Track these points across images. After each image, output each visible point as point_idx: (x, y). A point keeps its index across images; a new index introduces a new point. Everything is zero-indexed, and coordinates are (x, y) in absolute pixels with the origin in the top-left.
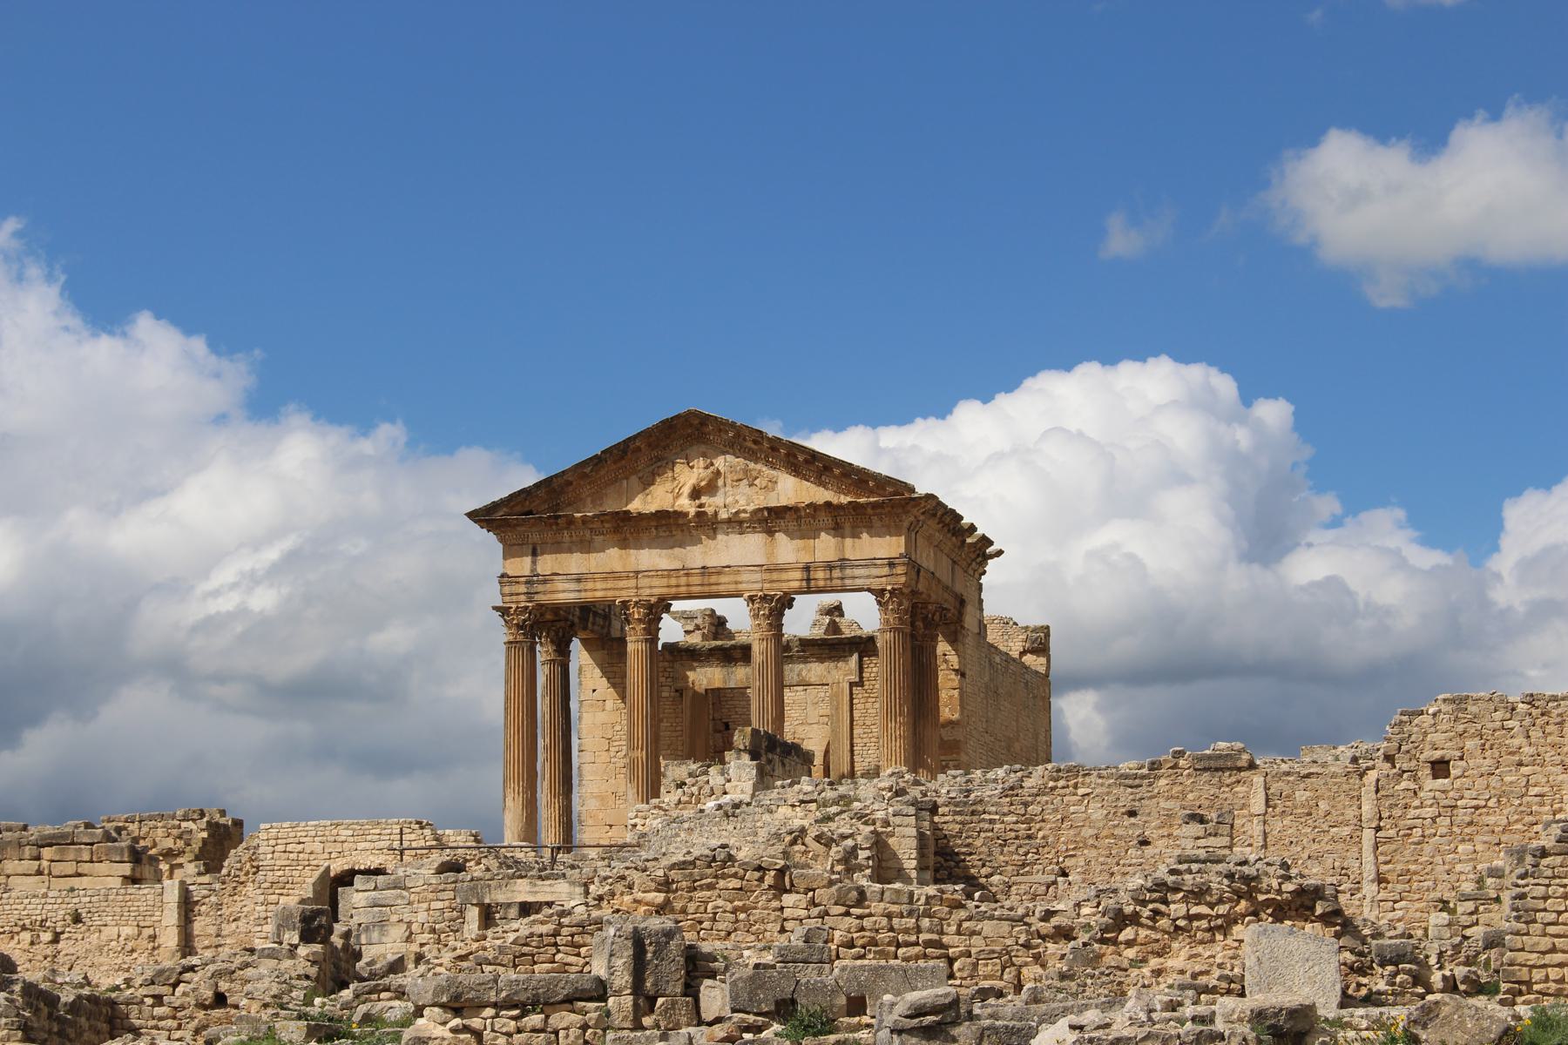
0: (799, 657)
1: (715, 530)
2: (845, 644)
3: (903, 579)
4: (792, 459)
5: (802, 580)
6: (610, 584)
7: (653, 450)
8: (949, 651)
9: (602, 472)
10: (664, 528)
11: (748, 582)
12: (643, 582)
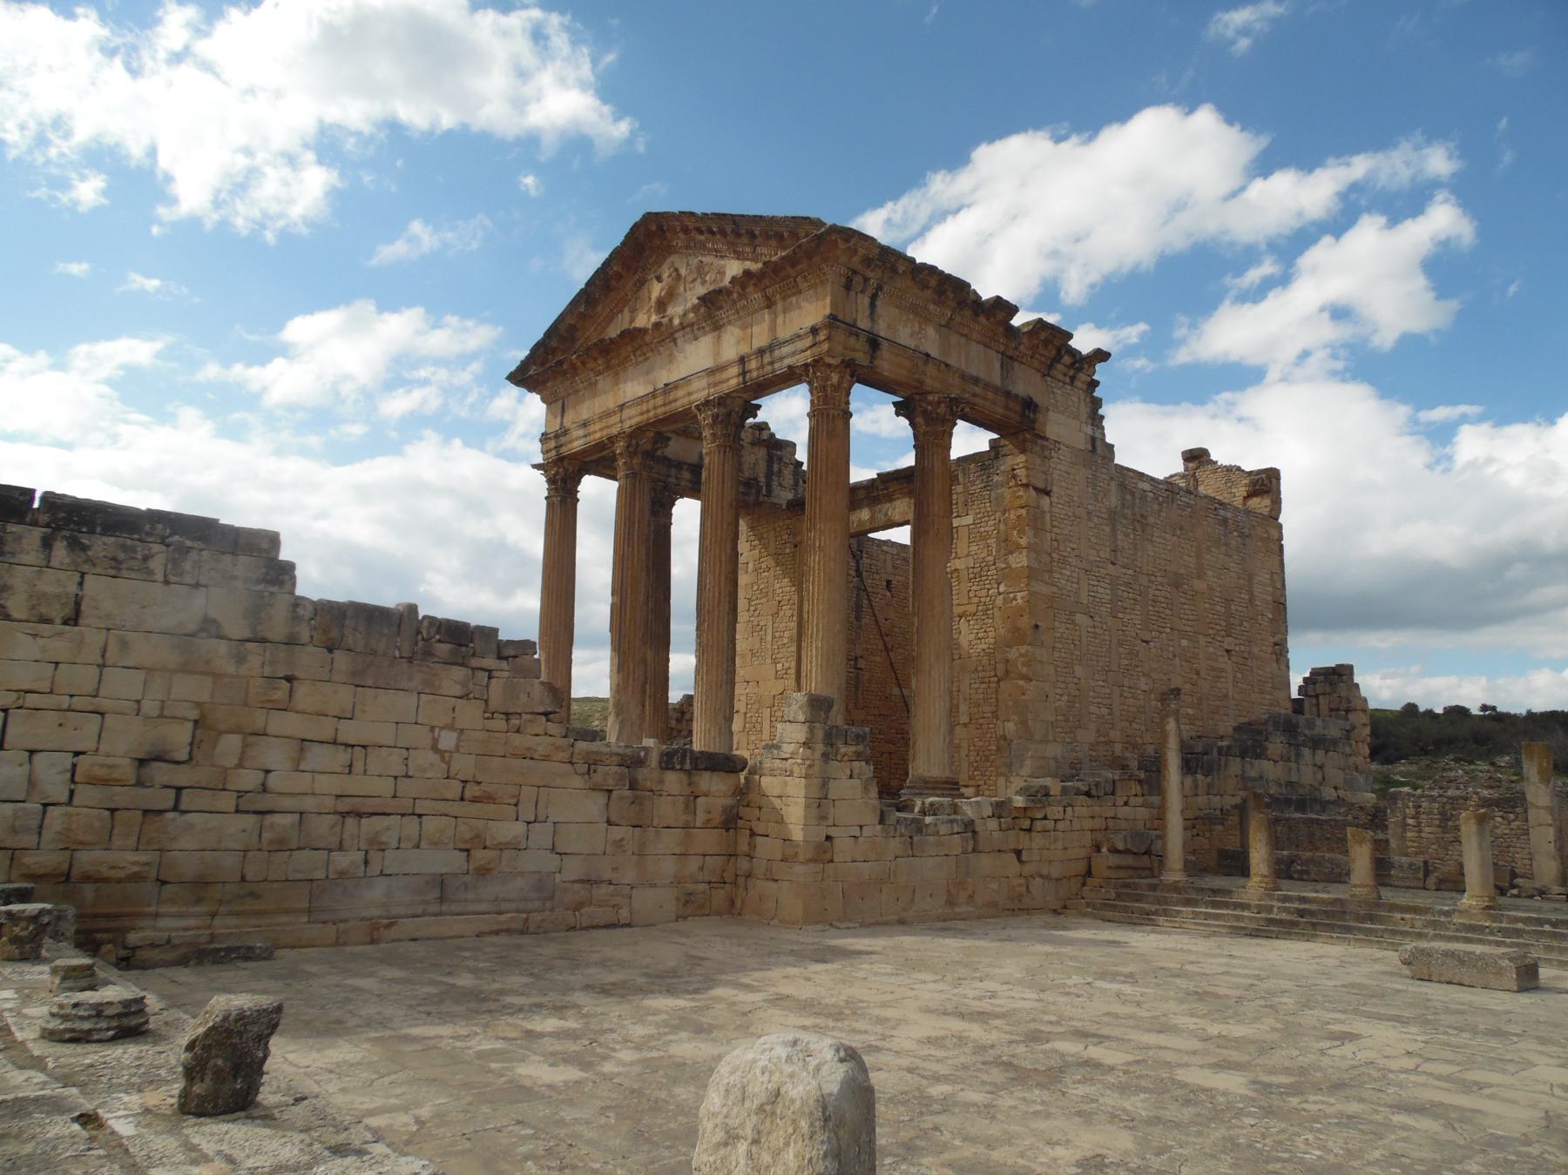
0: (884, 497)
1: (675, 340)
3: (825, 346)
7: (634, 274)
8: (1018, 464)
9: (599, 308)
10: (638, 353)
12: (626, 413)
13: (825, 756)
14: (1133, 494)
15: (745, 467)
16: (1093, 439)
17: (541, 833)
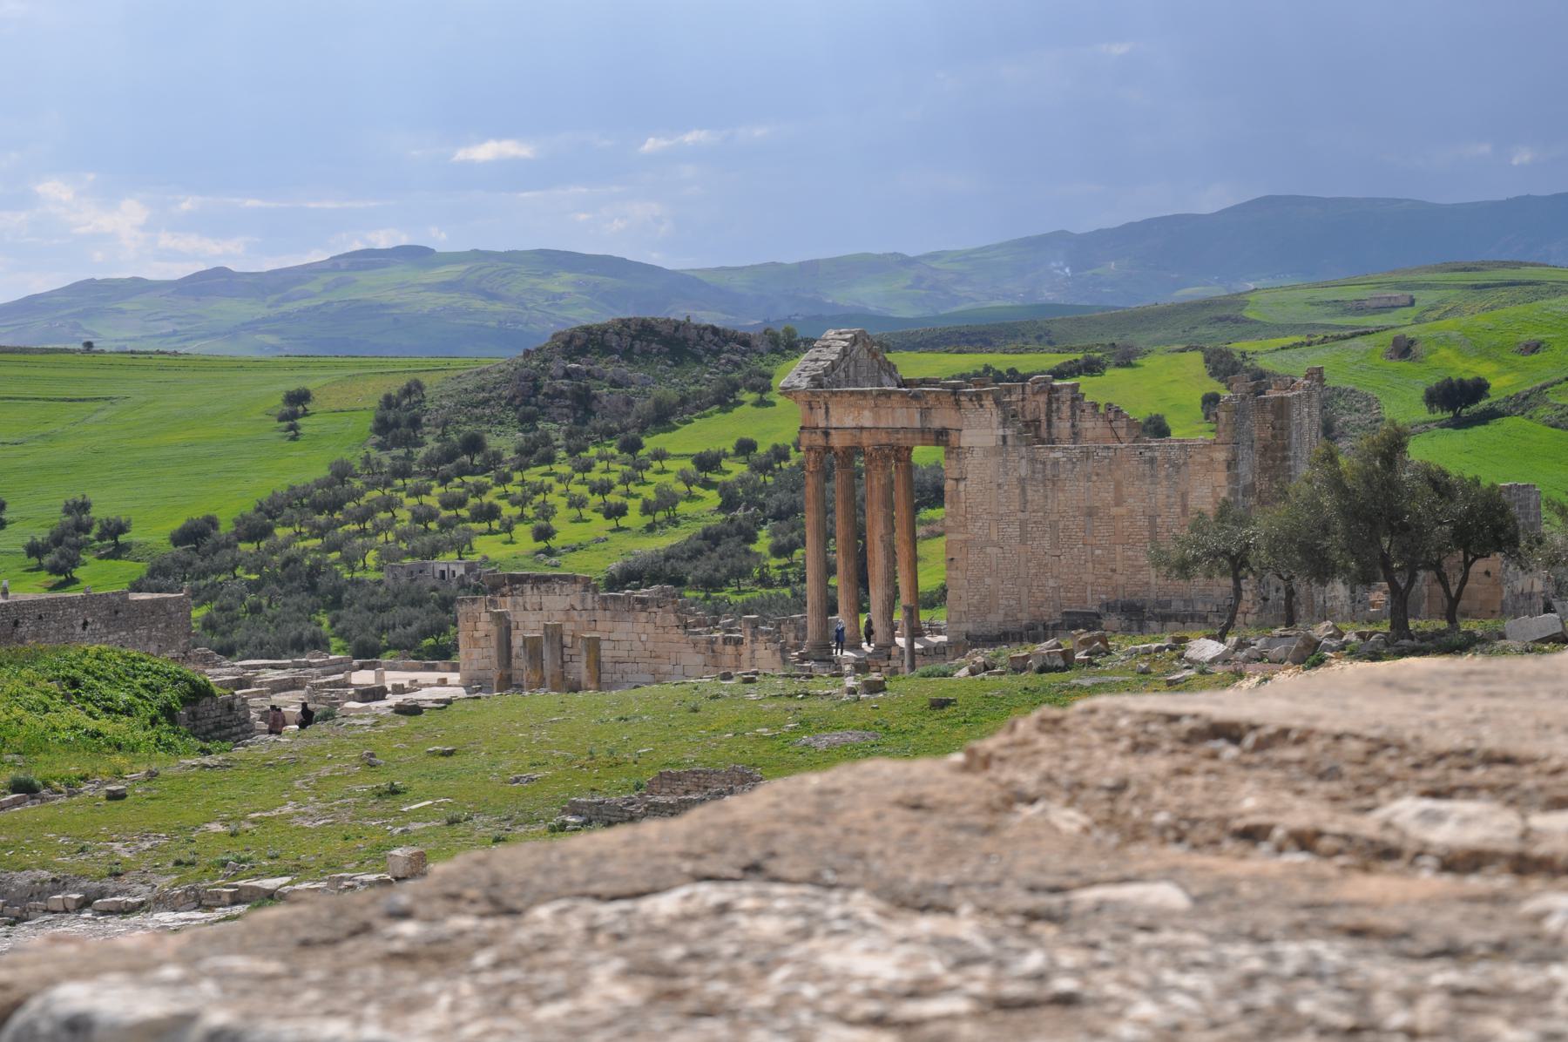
13: (752, 641)
14: (1044, 463)
15: (1027, 413)
16: (1004, 438)
17: (679, 669)
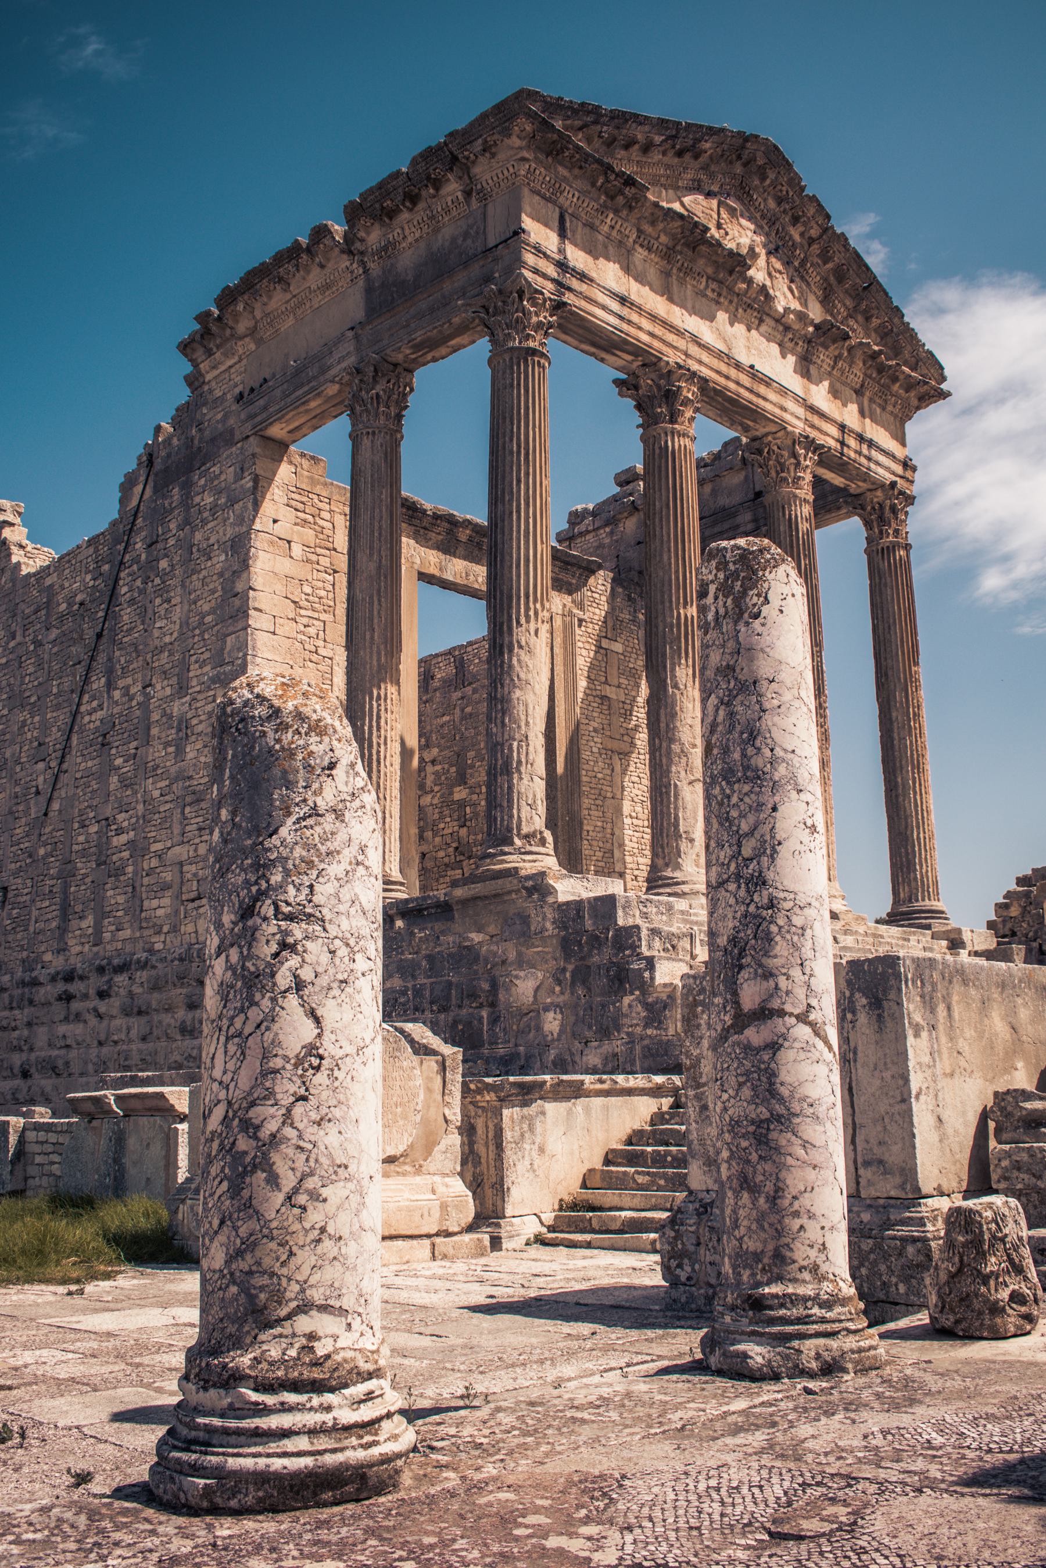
1: (761, 321)
2: (580, 567)
4: (832, 279)
5: (837, 440)
6: (658, 331)
10: (714, 285)
11: (792, 414)
